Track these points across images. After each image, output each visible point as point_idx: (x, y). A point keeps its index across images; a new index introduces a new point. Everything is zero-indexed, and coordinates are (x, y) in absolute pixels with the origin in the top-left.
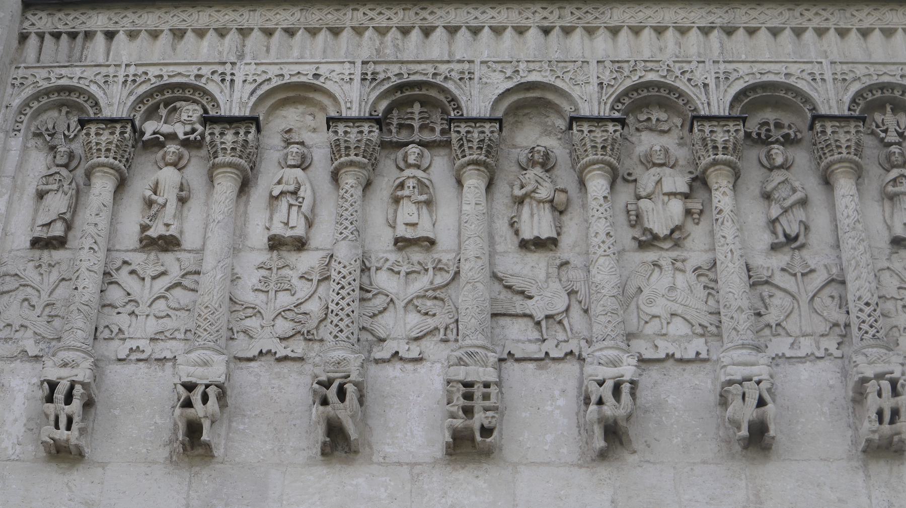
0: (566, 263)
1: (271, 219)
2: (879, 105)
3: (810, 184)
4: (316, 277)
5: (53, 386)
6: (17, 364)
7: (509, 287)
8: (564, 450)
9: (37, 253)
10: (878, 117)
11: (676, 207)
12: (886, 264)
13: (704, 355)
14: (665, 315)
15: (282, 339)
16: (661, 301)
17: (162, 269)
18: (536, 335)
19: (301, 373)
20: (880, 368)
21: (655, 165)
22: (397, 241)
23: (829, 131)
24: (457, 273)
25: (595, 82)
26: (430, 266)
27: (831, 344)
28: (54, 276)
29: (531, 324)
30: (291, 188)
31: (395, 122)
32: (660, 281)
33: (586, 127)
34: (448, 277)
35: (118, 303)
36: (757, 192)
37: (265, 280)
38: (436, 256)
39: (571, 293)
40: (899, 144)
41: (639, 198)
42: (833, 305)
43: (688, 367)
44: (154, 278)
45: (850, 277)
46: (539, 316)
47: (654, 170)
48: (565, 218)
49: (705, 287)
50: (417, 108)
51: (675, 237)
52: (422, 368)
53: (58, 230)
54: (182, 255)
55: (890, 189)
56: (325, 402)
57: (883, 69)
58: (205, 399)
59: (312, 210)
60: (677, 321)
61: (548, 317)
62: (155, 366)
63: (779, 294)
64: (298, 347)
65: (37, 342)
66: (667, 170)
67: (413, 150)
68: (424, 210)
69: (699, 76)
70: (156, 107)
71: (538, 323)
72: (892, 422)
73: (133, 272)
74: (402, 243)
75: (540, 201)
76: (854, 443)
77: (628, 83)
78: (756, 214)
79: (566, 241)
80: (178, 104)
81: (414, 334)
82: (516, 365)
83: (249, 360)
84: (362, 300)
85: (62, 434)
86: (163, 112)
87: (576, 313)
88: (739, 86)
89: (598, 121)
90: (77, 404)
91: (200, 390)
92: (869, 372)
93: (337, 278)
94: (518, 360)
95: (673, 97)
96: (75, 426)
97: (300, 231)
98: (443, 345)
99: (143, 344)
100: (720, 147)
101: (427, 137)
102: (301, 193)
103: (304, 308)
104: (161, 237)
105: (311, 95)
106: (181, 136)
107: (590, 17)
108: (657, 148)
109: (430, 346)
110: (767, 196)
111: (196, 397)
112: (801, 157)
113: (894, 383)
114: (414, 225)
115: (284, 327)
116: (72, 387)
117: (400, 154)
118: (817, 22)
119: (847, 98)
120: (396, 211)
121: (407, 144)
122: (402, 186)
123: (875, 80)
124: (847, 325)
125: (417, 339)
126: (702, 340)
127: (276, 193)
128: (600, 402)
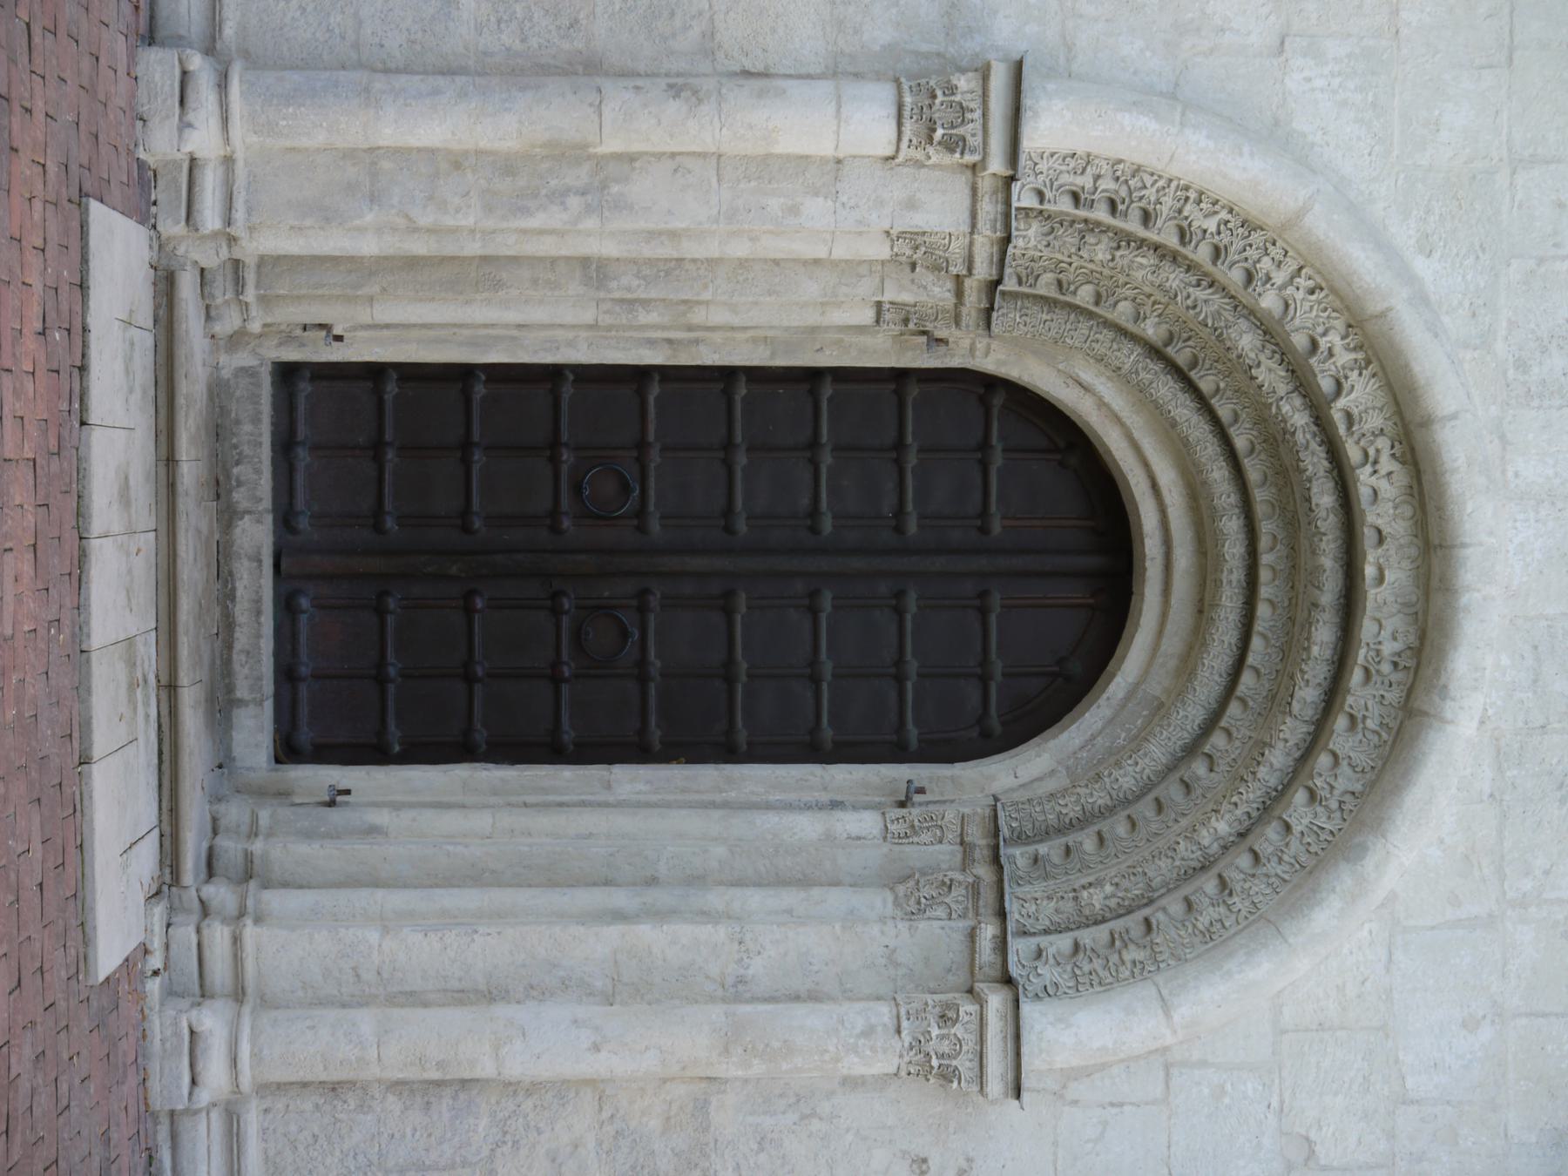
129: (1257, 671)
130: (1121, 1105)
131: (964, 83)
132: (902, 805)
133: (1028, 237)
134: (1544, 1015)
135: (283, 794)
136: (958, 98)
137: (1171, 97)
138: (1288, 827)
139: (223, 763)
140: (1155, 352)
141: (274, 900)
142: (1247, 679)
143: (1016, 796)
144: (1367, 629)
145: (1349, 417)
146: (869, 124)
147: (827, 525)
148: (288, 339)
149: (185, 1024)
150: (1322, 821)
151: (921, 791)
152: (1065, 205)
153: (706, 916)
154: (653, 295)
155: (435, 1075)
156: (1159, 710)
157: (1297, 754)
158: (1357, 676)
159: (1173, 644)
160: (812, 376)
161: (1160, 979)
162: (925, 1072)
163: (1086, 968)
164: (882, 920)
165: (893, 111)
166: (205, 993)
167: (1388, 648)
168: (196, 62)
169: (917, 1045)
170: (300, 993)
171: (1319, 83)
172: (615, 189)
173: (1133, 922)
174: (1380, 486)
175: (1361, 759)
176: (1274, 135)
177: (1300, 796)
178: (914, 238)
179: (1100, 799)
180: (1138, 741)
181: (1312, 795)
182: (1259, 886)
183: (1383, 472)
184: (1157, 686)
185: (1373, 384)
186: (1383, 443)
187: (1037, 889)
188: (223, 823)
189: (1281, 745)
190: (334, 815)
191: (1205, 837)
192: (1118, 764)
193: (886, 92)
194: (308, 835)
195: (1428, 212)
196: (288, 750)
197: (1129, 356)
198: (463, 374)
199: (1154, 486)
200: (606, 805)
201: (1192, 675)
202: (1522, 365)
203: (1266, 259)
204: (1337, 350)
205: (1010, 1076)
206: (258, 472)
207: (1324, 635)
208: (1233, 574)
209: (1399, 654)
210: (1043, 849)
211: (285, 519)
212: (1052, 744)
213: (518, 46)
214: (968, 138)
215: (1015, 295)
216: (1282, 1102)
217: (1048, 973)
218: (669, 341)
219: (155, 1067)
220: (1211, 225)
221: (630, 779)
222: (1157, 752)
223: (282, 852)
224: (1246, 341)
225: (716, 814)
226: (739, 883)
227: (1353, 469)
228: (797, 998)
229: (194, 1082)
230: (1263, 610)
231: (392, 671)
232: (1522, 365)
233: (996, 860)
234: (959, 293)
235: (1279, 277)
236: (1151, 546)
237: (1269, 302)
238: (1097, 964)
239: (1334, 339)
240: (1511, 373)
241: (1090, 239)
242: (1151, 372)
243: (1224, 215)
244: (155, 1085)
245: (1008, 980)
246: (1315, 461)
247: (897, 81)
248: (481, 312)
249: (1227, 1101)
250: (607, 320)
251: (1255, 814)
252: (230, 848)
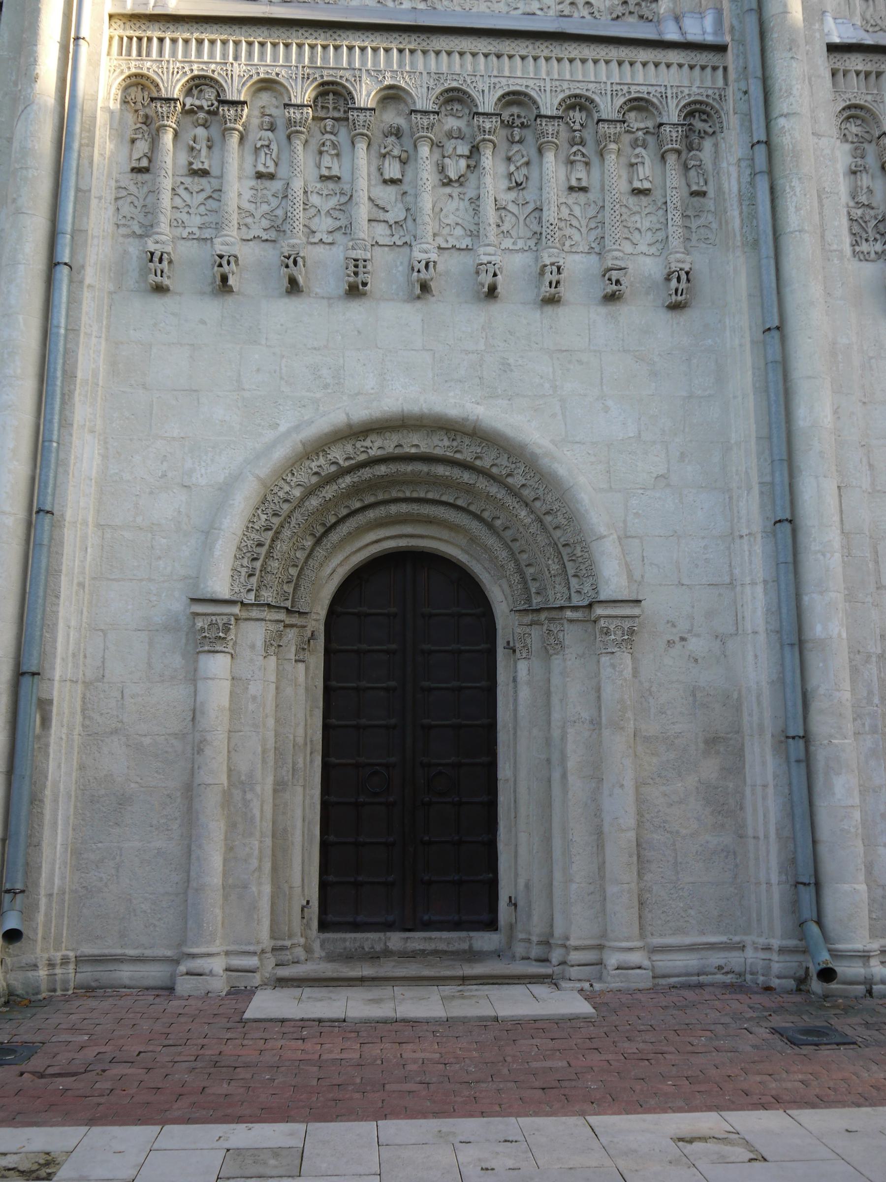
0: (405, 193)
1: (256, 160)
2: (572, 107)
3: (533, 152)
4: (280, 196)
5: (152, 254)
6: (131, 240)
7: (377, 205)
8: (401, 294)
9: (135, 175)
10: (571, 113)
11: (463, 163)
12: (564, 201)
13: (470, 247)
14: (453, 224)
15: (265, 230)
16: (452, 216)
17: (201, 187)
18: (389, 232)
19: (274, 249)
20: (553, 260)
21: (453, 137)
22: (321, 177)
23: (544, 124)
24: (351, 196)
25: (425, 86)
26: (338, 192)
27: (531, 243)
28: (145, 190)
29: (387, 227)
30: (266, 143)
31: (320, 105)
32: (452, 205)
33: (419, 116)
34: (347, 198)
35: (179, 206)
36: (504, 156)
37: (254, 196)
38: (341, 186)
39: (408, 210)
40: (580, 131)
41: (444, 157)
42: (535, 222)
43: (462, 253)
44: (197, 192)
45: (544, 209)
46: (391, 222)
47: (453, 141)
48: (406, 166)
49: (474, 209)
50: (331, 96)
51: (461, 181)
52: (334, 249)
53: (144, 163)
54: (212, 180)
55: (572, 158)
56: (287, 266)
57: (578, 85)
58: (229, 263)
59: (278, 157)
60: (459, 227)
61: (396, 223)
62: (202, 242)
63: (510, 215)
64: (273, 235)
65: (140, 227)
66: (460, 141)
67: (329, 122)
68: (335, 159)
69: (480, 86)
70: (191, 89)
71: (391, 226)
72: (556, 287)
73: (186, 189)
74: (324, 178)
75: (394, 157)
76: (538, 295)
77: (443, 88)
78: (502, 168)
79: (406, 180)
80: (203, 87)
81: (330, 230)
82: (379, 248)
83: (248, 240)
84: (304, 209)
85: (159, 279)
86: (195, 92)
87: (410, 221)
88: (500, 93)
89: (426, 113)
90: (165, 263)
91: (226, 258)
92: (548, 263)
93: (292, 198)
94: (380, 246)
95: (465, 97)
96: (164, 275)
97: (272, 170)
98: (343, 236)
99: (195, 230)
100: (487, 130)
101: (336, 115)
102: (272, 147)
103: (275, 213)
104: (200, 169)
105: (274, 85)
106: (206, 108)
107: (425, 44)
108: (455, 128)
109: (338, 236)
110: (509, 159)
111: (224, 263)
112: (528, 134)
113: (559, 268)
114: (329, 168)
115: (265, 223)
116: (162, 255)
117: (322, 124)
118: (546, 53)
119: (556, 102)
120: (320, 159)
121: (326, 119)
122: (323, 144)
123: (573, 92)
124: (541, 234)
125: (331, 232)
126: (470, 239)
127: (258, 146)
128: (419, 271)
129: (456, 498)
130: (643, 557)
131: (199, 624)
132: (514, 651)
133: (268, 596)
134: (602, 379)
135: (512, 927)
136: (206, 626)
137: (208, 534)
138: (523, 485)
139: (498, 954)
140: (318, 541)
141: (558, 931)
142: (459, 502)
143: (511, 602)
144: (438, 452)
146: (217, 665)
147: (392, 684)
148: (308, 926)
149: (614, 972)
151: (508, 643)
152: (254, 580)
153: (563, 738)
154: (291, 761)
155: (635, 858)
156: (473, 540)
157: (492, 481)
158: (458, 456)
159: (445, 534)
160: (327, 690)
161: (589, 540)
162: (630, 641)
163: (584, 572)
164: (564, 660)
165: (211, 655)
166: (600, 963)
167: (446, 443)
168: (182, 968)
169: (619, 645)
170: (600, 919)
171: (203, 471)
172: (243, 778)
173: (565, 552)
174: (376, 446)
175: (494, 454)
176: (226, 489)
177: (510, 480)
178: (267, 645)
179: (511, 565)
180: (486, 549)
181: (509, 475)
182: (549, 498)
183: (371, 445)
184: (464, 542)
185: (333, 448)
186: (358, 444)
187: (550, 593)
188: (524, 954)
189: (488, 488)
190: (520, 904)
191: (528, 521)
192: (497, 558)
193: (203, 658)
194: (529, 916)
195: (259, 425)
196: (492, 925)
197: (320, 552)
198: (325, 847)
200: (515, 780)
201: (458, 526)
202: (326, 386)
203: (279, 494)
204: (319, 464)
206: (367, 939)
207: (441, 470)
208: (414, 508)
210: (533, 590)
211: (388, 927)
212: (488, 586)
213: (178, 821)
215: (293, 602)
216: (641, 488)
217: (587, 588)
218: (311, 753)
219: (634, 986)
221: (504, 771)
222: (491, 541)
223: (537, 928)
224: (314, 502)
225: (519, 733)
226: (549, 723)
227: (370, 457)
228: (599, 697)
229: (640, 968)
230: (430, 496)
231: (456, 878)
232: (326, 386)
233: (538, 611)
234: (292, 626)
235: (287, 488)
236: (402, 543)
237: (297, 493)
238: (583, 567)
239: (313, 465)
240: (329, 391)
241: (269, 569)
242: (327, 543)
243: (259, 512)
244: (641, 986)
245: (590, 606)
246: (366, 473)
247: (198, 653)
248: (297, 837)
250: (301, 782)
251: (518, 500)
252: (535, 951)
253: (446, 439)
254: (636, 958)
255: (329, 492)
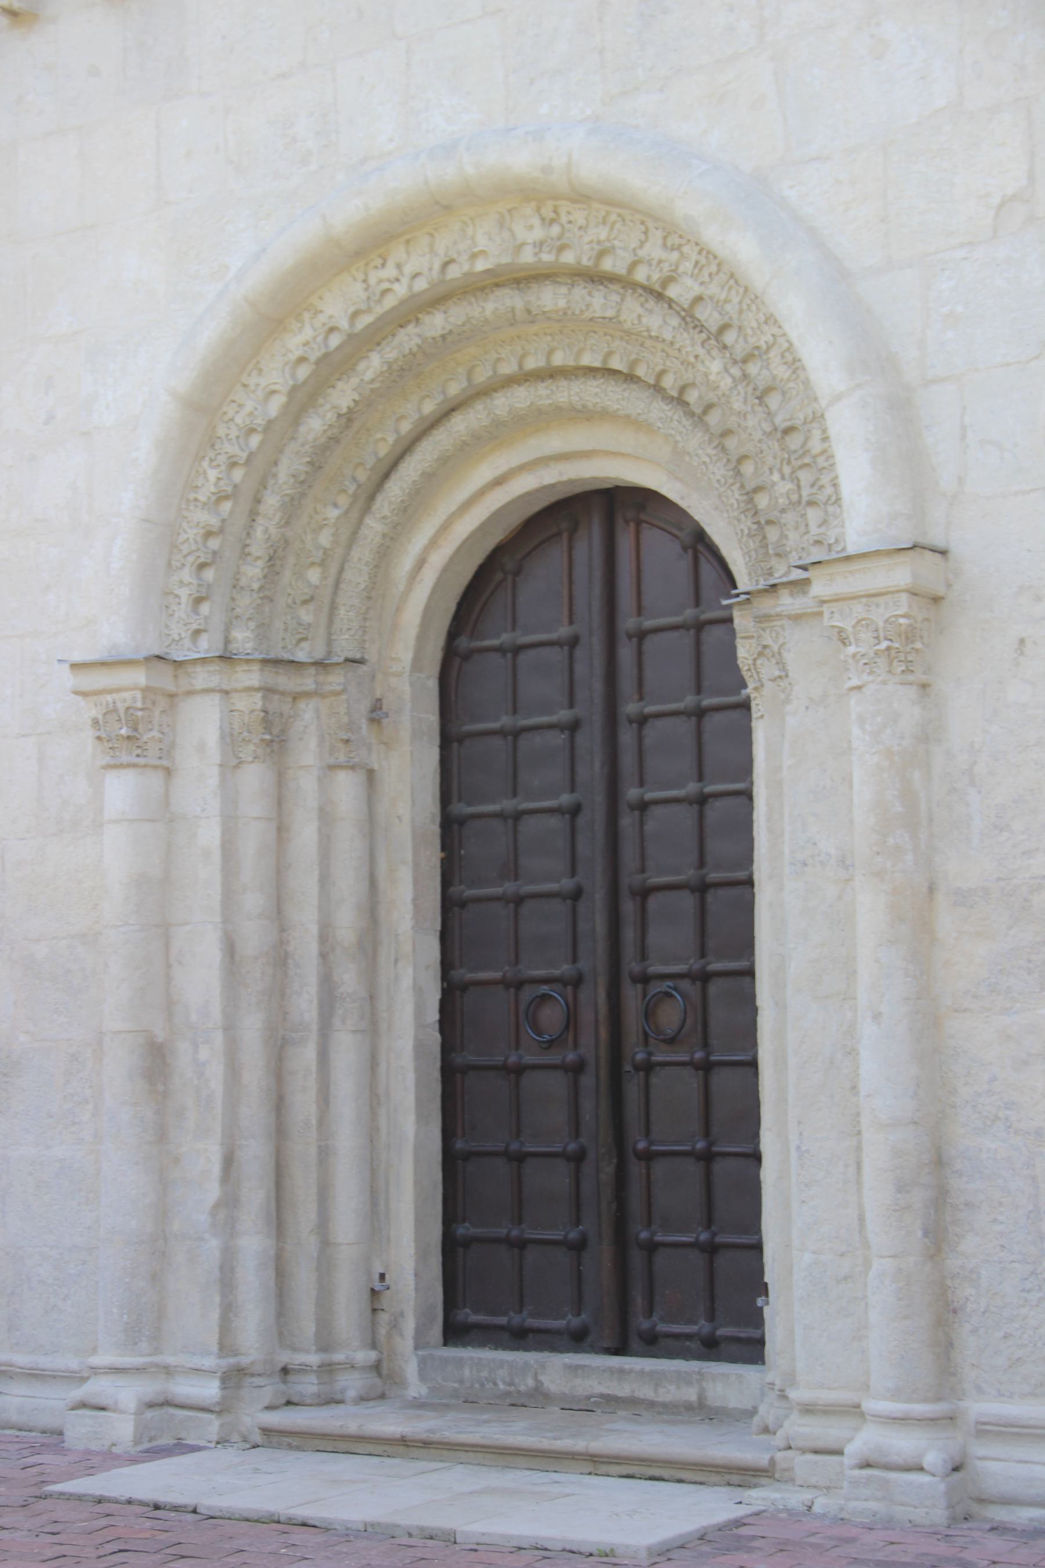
136: (100, 717)
138: (699, 299)
144: (527, 257)
145: (355, 315)
149: (857, 1472)
150: (687, 266)
158: (568, 258)
172: (194, 1017)
174: (412, 269)
199: (499, 482)
205: (886, 561)
206: (502, 1364)
209: (543, 219)
214: (127, 705)
218: (396, 961)
220: (212, 474)
234: (307, 695)
243: (205, 464)
246: (408, 338)
249: (959, 309)
253: (536, 221)
254: (903, 1444)
255: (343, 396)
